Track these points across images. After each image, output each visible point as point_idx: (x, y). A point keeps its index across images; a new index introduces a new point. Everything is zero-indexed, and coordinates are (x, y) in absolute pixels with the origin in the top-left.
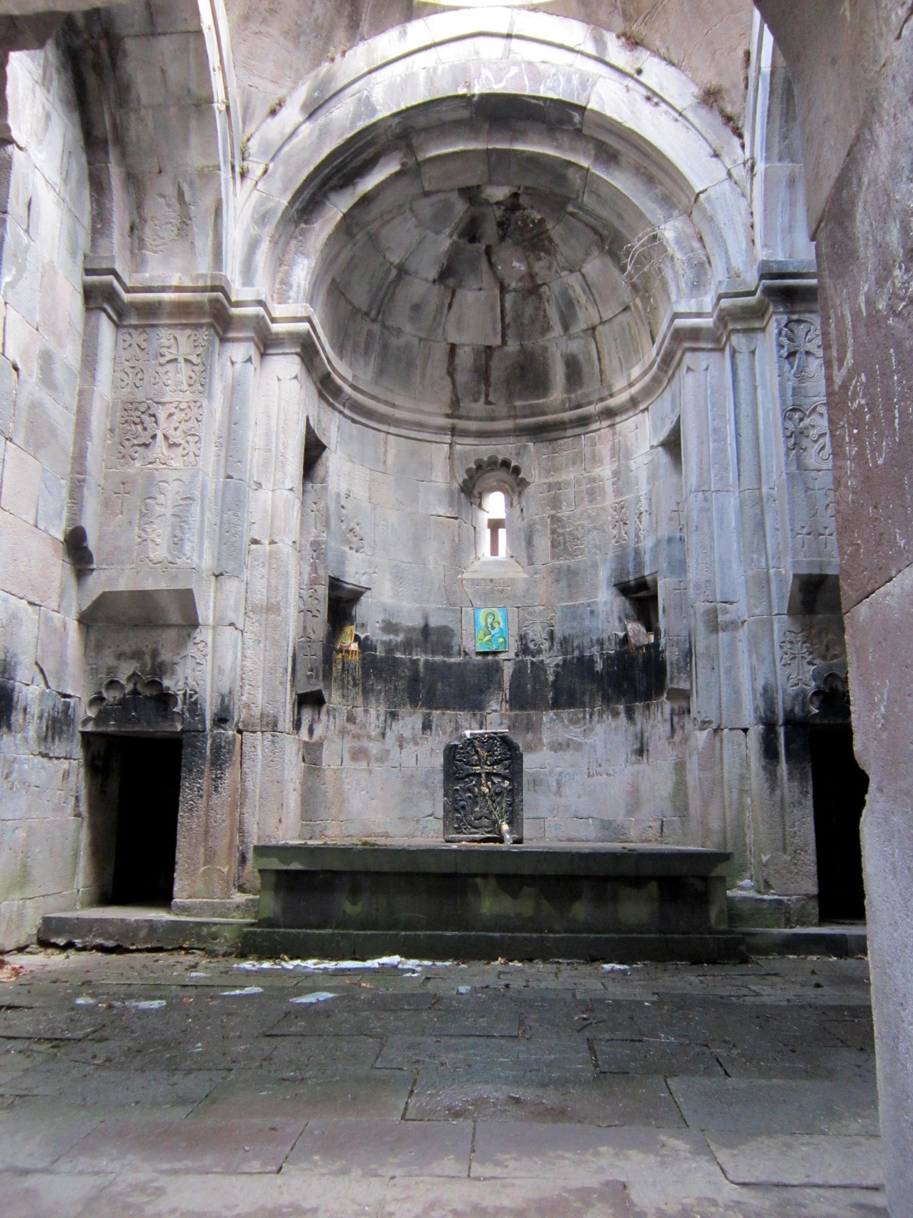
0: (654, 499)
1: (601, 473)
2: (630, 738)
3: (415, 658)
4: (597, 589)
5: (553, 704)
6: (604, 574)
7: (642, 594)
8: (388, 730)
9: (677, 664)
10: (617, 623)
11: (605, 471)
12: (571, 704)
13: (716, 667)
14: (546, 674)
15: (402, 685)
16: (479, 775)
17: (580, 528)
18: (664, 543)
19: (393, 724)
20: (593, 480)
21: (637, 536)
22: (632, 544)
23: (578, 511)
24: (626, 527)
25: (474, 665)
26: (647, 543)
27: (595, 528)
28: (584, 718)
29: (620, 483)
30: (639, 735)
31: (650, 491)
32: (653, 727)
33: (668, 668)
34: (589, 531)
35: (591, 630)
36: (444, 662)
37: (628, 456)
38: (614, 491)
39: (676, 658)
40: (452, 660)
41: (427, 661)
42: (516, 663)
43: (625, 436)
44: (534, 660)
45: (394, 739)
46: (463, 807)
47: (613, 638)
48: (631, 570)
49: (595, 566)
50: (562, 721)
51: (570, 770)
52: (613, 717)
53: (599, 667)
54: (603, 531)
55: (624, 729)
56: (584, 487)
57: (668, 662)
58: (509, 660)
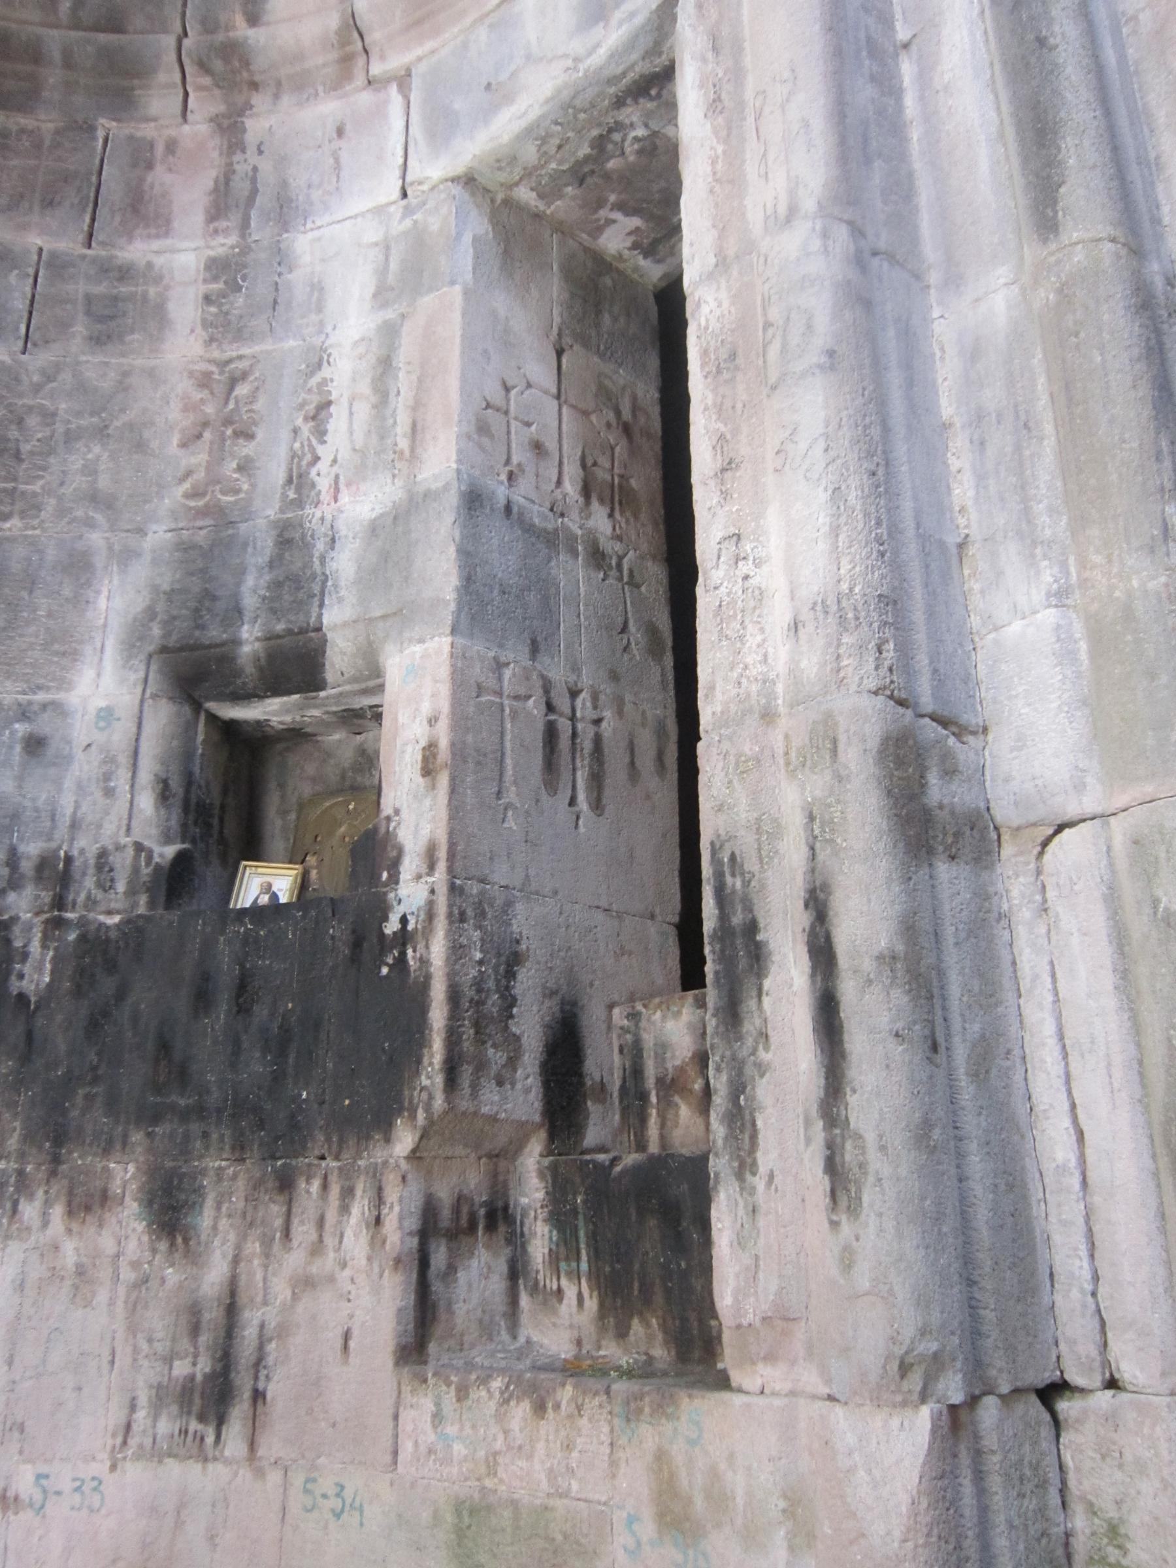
0: (407, 351)
1: (159, 261)
2: (158, 1321)
4: (73, 655)
6: (117, 602)
7: (272, 711)
9: (478, 1004)
10: (146, 802)
11: (180, 255)
13: (941, 1039)
17: (32, 421)
18: (452, 499)
20: (125, 273)
21: (299, 482)
22: (269, 510)
23: (39, 360)
24: (247, 449)
26: (354, 507)
27: (101, 433)
29: (240, 300)
30: (212, 1315)
31: (390, 333)
32: (305, 1284)
33: (438, 1016)
34: (70, 437)
35: (15, 816)
37: (287, 211)
38: (205, 324)
39: (473, 973)
43: (282, 161)
47: (123, 862)
48: (250, 601)
49: (79, 567)
52: (70, 1213)
53: (36, 973)
54: (140, 446)
55: (128, 1275)
56: (80, 288)
57: (438, 991)
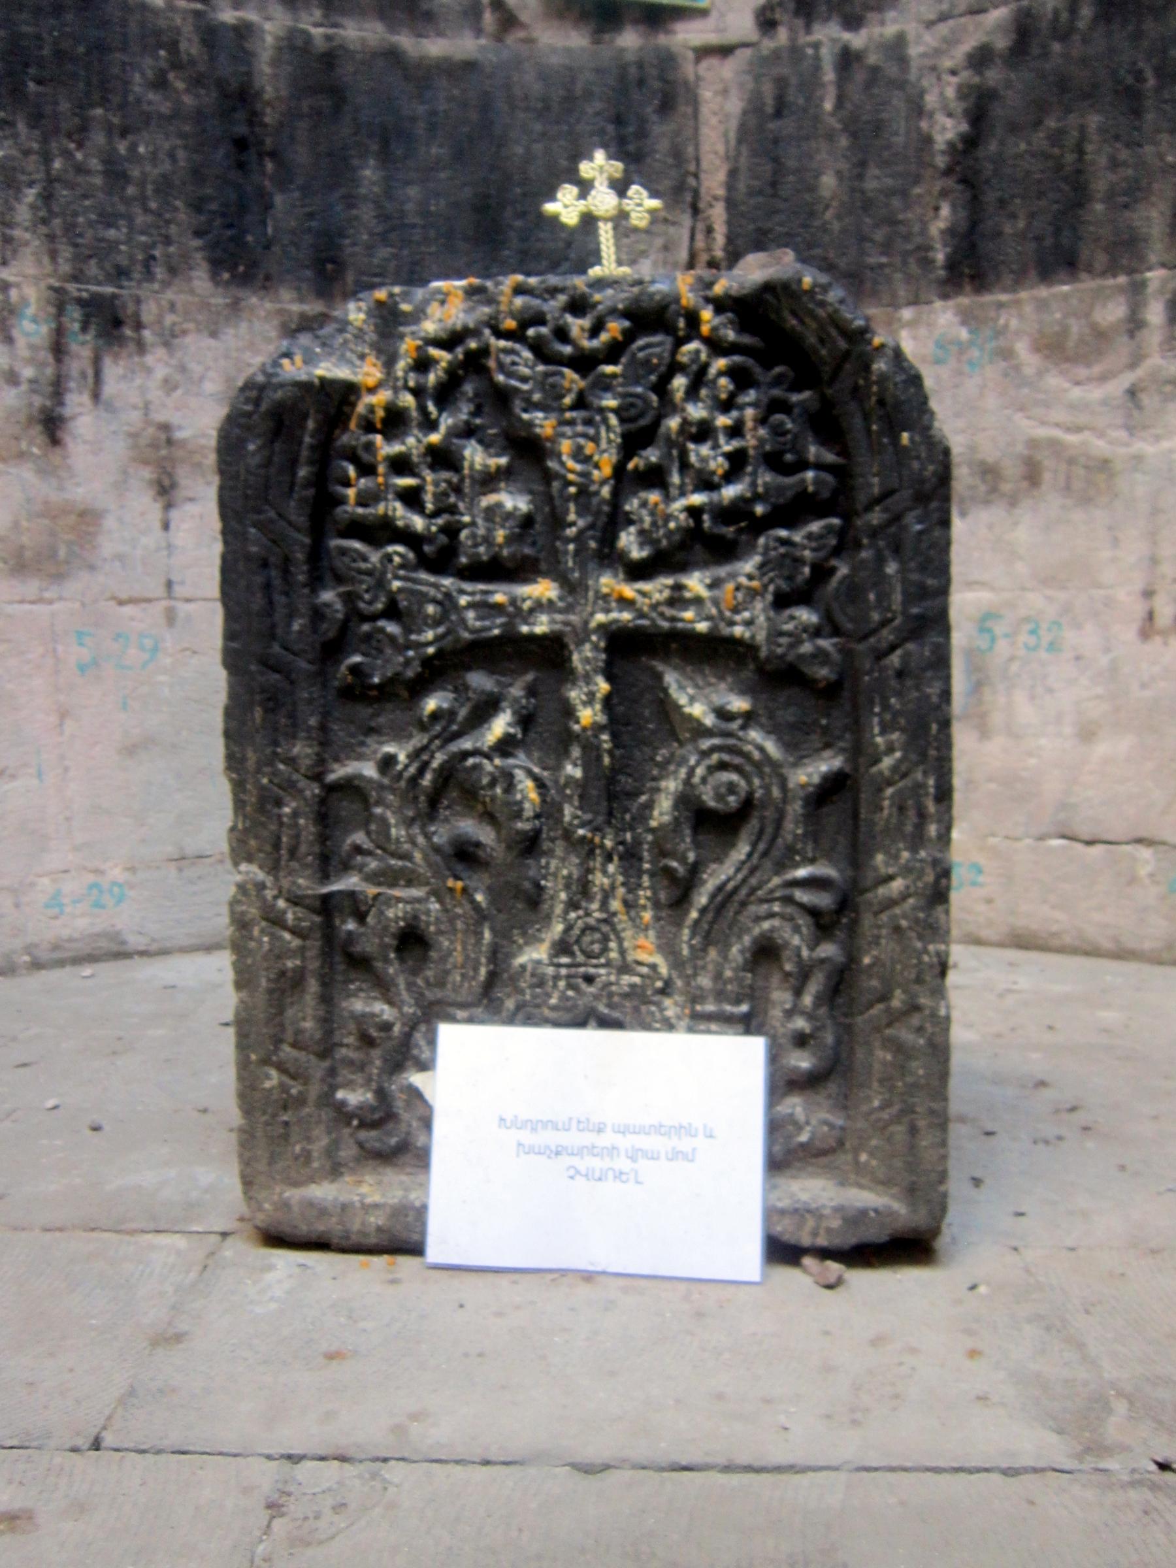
3: (228, 16)
5: (952, 265)
8: (77, 402)
12: (1059, 260)
14: (918, 110)
15: (155, 153)
16: (550, 655)
19: (113, 371)
25: (544, 75)
28: (1135, 324)
36: (393, 55)
40: (435, 47)
41: (295, 46)
42: (762, 65)
44: (857, 40)
45: (118, 449)
46: (412, 941)
50: (1006, 354)
51: (1035, 601)
58: (725, 51)
